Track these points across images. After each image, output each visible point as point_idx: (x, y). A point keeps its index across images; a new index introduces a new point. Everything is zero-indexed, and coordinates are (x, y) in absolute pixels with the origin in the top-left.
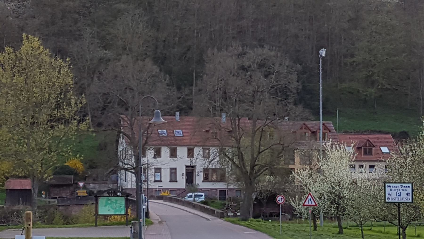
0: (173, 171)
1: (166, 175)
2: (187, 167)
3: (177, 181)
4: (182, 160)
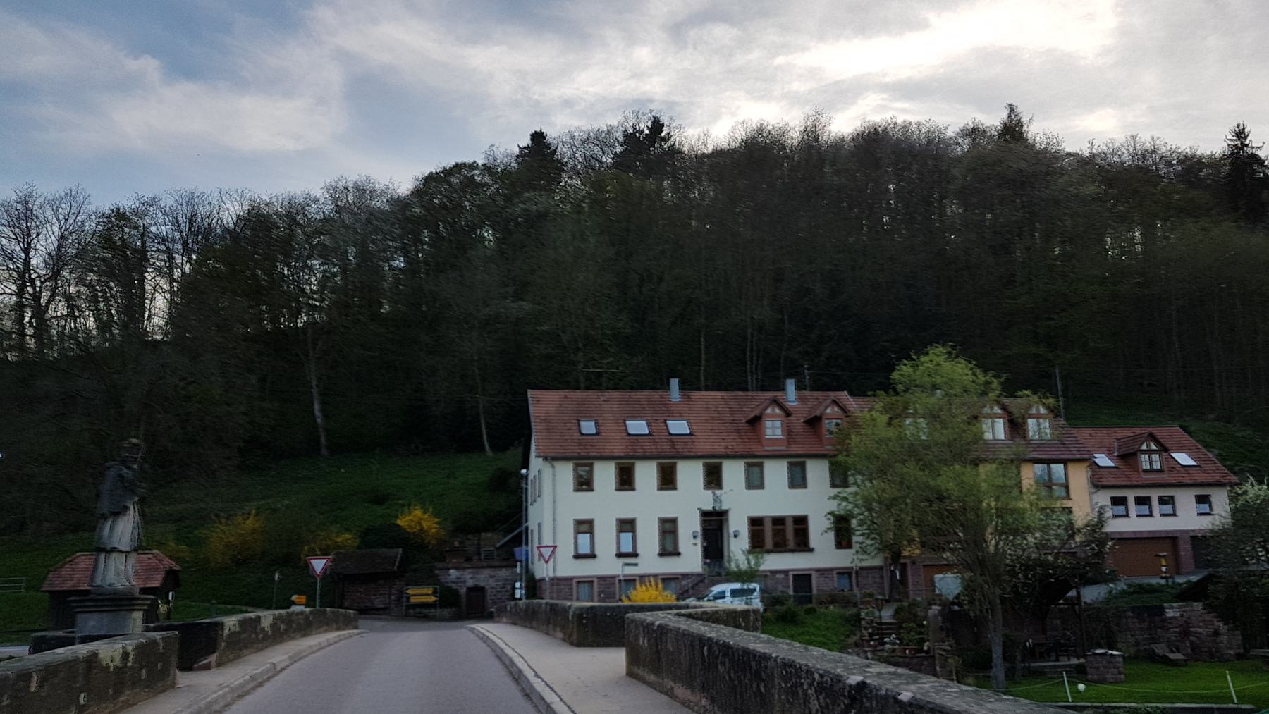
0: (669, 528)
1: (649, 538)
2: (705, 514)
3: (678, 554)
4: (690, 497)
